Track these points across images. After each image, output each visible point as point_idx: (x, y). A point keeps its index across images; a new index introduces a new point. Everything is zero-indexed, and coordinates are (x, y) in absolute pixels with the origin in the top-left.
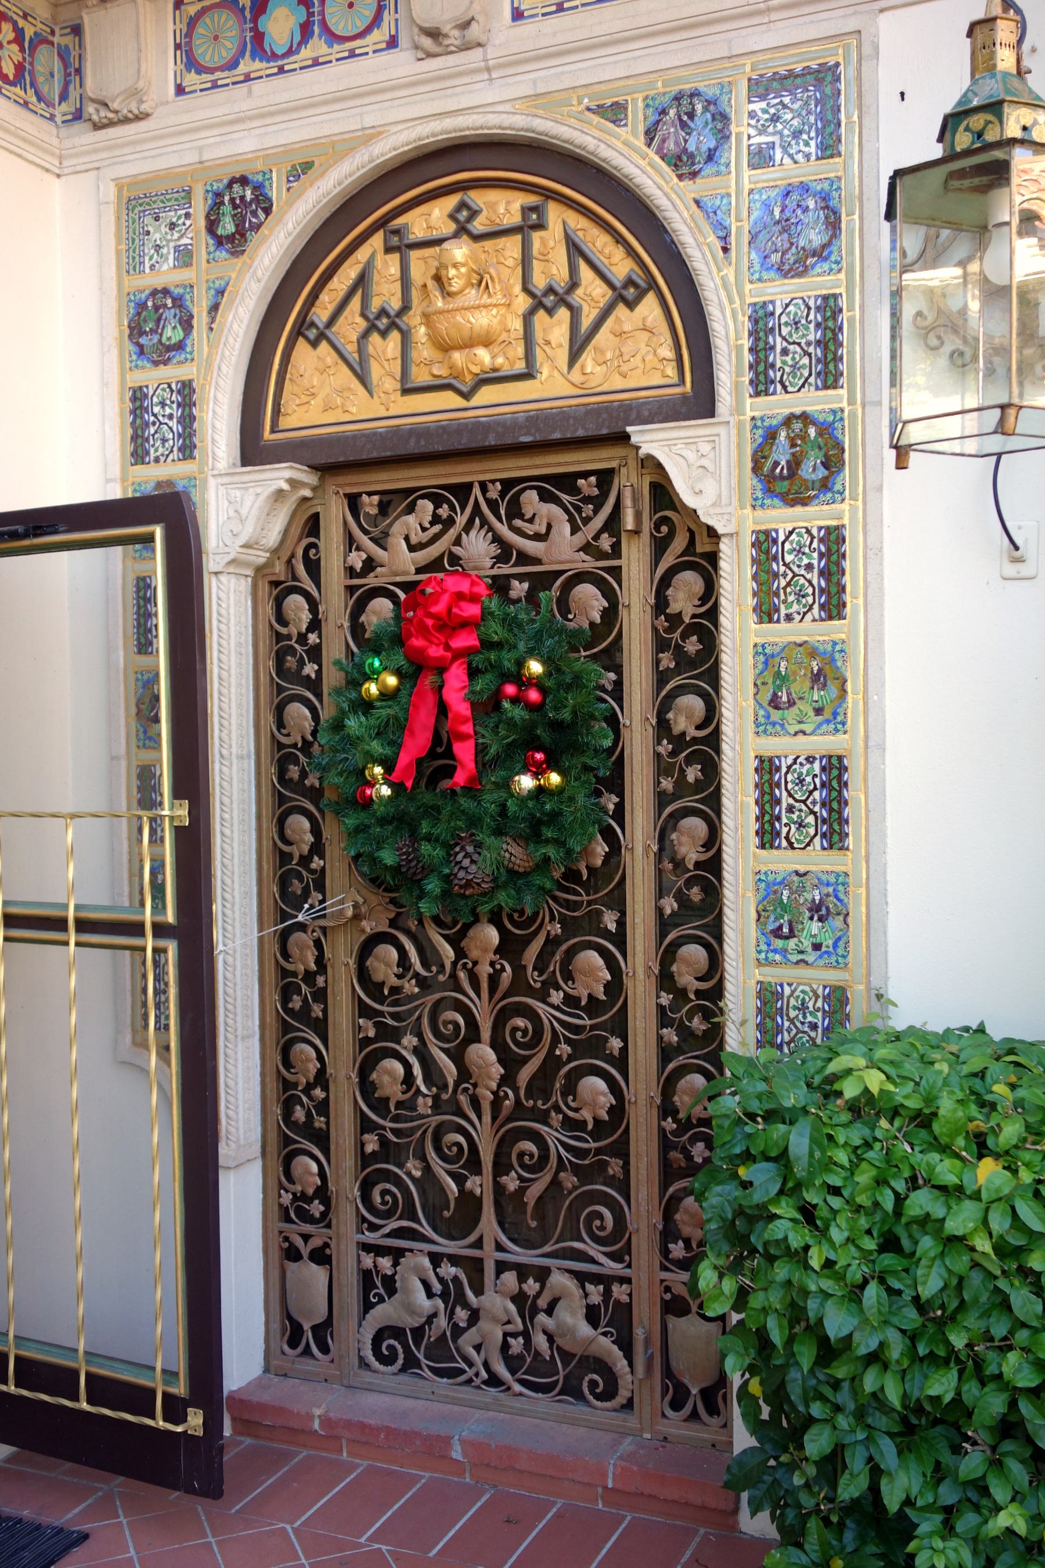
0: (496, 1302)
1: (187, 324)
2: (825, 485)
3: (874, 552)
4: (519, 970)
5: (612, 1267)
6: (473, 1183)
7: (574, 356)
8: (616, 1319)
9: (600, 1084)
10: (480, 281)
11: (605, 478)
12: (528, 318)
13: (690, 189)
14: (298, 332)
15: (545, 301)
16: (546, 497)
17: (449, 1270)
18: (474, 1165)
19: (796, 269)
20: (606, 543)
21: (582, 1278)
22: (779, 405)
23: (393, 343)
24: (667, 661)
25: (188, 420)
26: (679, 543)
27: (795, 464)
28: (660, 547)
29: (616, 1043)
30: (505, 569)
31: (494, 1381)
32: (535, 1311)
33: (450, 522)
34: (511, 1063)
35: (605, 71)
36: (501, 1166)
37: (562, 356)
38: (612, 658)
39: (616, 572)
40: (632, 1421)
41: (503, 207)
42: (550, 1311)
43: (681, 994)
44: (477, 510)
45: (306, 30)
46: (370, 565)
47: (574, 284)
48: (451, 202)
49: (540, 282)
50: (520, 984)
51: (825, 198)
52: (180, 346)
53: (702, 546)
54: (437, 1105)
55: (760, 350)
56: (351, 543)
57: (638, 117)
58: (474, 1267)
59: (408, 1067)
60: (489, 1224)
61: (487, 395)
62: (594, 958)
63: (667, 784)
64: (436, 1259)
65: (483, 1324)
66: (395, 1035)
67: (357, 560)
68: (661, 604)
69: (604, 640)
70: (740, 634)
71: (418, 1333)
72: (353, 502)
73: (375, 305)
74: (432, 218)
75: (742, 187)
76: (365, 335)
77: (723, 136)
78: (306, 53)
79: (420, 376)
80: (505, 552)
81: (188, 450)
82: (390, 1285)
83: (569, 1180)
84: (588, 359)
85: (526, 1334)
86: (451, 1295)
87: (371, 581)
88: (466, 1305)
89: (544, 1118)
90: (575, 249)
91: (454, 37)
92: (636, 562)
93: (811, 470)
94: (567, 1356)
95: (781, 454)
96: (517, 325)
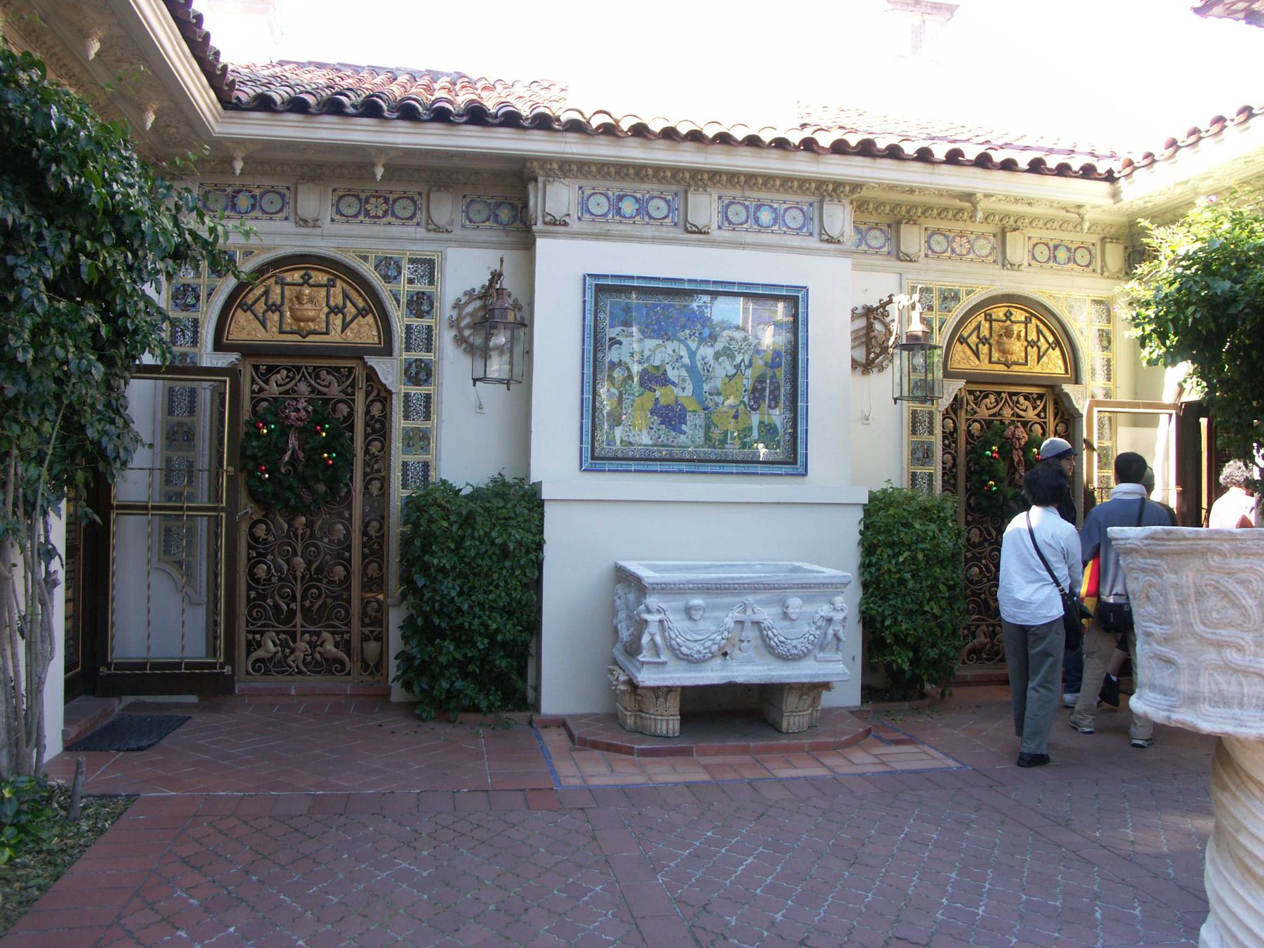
0: (302, 645)
1: (198, 298)
2: (426, 381)
3: (439, 403)
4: (312, 532)
5: (345, 629)
6: (293, 606)
7: (343, 330)
8: (345, 646)
9: (341, 568)
10: (311, 301)
11: (351, 370)
12: (327, 315)
13: (389, 287)
14: (240, 306)
15: (335, 310)
16: (328, 373)
17: (283, 636)
18: (294, 599)
19: (420, 315)
20: (350, 390)
21: (333, 633)
22: (413, 355)
23: (276, 316)
24: (369, 430)
25: (196, 333)
26: (375, 393)
27: (417, 373)
28: (368, 394)
29: (347, 554)
30: (313, 396)
31: (300, 672)
32: (316, 646)
33: (293, 378)
34: (309, 563)
35: (363, 245)
36: (304, 598)
37: (339, 329)
38: (351, 428)
39: (353, 400)
40: (350, 678)
41: (323, 278)
42: (321, 646)
43: (370, 538)
44: (303, 375)
45: (253, 207)
46: (261, 390)
47: (345, 306)
48: (302, 272)
49: (332, 304)
50: (312, 536)
51: (429, 298)
52: (193, 306)
53: (383, 394)
54: (280, 579)
55: (408, 338)
56: (253, 381)
57: (372, 261)
58: (293, 635)
59: (269, 567)
60: (299, 619)
61: (311, 338)
62: (340, 527)
63: (368, 470)
64: (278, 633)
65: (297, 653)
66: (265, 556)
67: (256, 387)
68: (367, 412)
69: (349, 422)
70: (399, 424)
71: (270, 659)
72: (256, 368)
73: (270, 302)
74: (296, 276)
75: (404, 288)
76: (266, 311)
77: (400, 273)
78: (253, 214)
79: (287, 329)
80: (313, 390)
81: (195, 343)
82: (259, 645)
83: (329, 601)
84: (348, 332)
85: (312, 654)
86: (284, 645)
87: (261, 396)
88: (289, 647)
89: (320, 580)
90: (346, 296)
91: (311, 223)
92: (360, 397)
93: (422, 376)
94: (326, 660)
95: (413, 370)
96: (324, 317)
